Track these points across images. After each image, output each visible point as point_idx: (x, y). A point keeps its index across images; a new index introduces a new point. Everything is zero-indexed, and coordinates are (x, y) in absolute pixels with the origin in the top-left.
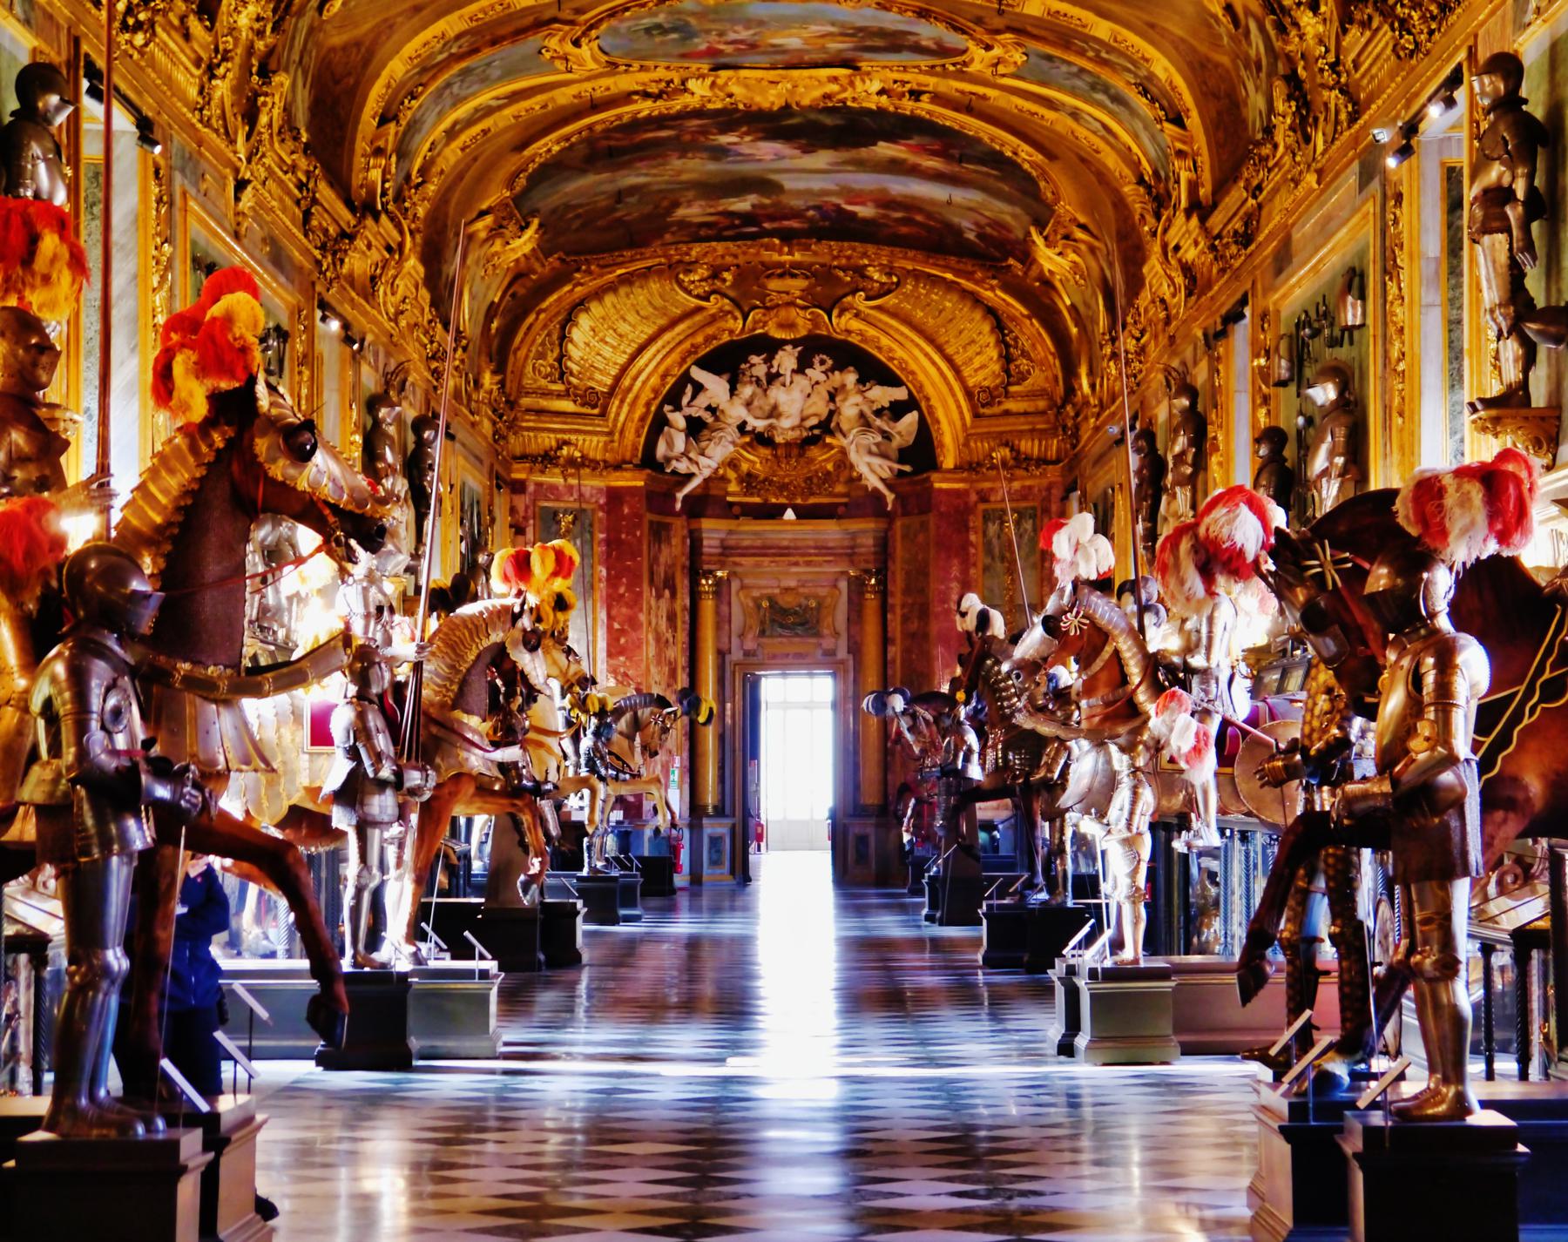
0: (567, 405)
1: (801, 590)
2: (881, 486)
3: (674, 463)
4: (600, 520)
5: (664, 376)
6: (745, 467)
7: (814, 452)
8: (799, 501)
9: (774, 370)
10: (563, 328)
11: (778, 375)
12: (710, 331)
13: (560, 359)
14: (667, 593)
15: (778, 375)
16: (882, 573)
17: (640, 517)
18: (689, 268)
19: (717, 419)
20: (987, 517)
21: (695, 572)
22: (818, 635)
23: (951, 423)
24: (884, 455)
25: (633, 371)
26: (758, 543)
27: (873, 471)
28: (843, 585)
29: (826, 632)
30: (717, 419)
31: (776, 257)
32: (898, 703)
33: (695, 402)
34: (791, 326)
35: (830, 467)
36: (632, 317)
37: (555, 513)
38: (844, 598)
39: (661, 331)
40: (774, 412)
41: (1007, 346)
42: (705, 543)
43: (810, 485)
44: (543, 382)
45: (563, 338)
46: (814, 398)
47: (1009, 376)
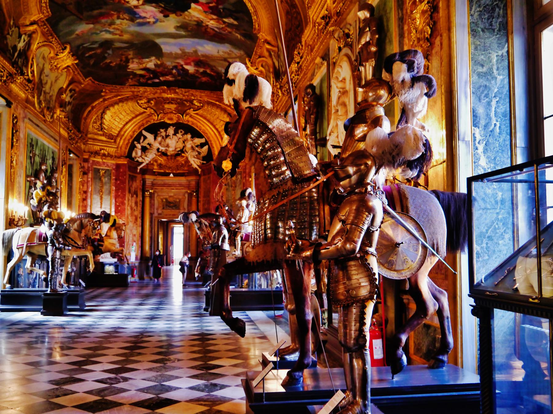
0: (103, 138)
2: (197, 167)
3: (137, 159)
5: (134, 132)
6: (159, 162)
7: (179, 158)
10: (102, 115)
11: (169, 135)
12: (148, 119)
13: (101, 124)
14: (135, 196)
16: (197, 192)
17: (126, 172)
18: (141, 98)
19: (151, 147)
21: (144, 191)
22: (179, 209)
23: (217, 148)
24: (198, 159)
25: (124, 130)
27: (195, 163)
28: (186, 195)
30: (151, 147)
31: (165, 95)
32: (194, 217)
34: (171, 119)
35: (183, 162)
36: (124, 113)
37: (99, 170)
38: (187, 199)
39: (133, 118)
40: (168, 146)
44: (96, 131)
45: (102, 118)
46: (179, 143)
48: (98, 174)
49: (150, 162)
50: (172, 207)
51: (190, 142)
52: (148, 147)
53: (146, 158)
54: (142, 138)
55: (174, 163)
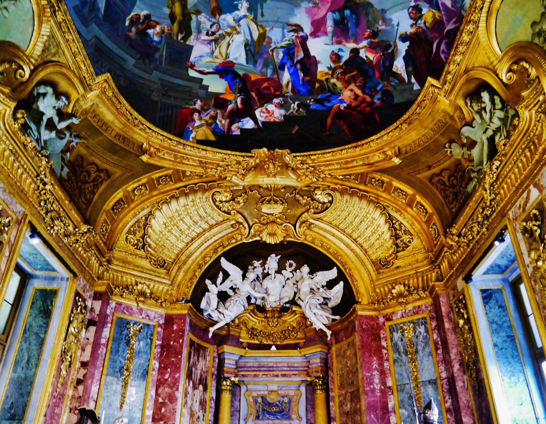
1: (280, 392)
4: (158, 333)
6: (251, 324)
8: (279, 343)
9: (266, 271)
11: (268, 274)
13: (143, 237)
14: (201, 387)
15: (268, 274)
19: (236, 293)
20: (392, 330)
23: (363, 281)
25: (187, 252)
27: (320, 320)
28: (303, 389)
29: (294, 416)
30: (236, 293)
33: (224, 284)
36: (188, 220)
37: (128, 323)
38: (304, 397)
41: (396, 229)
42: (226, 361)
43: (285, 334)
47: (397, 246)
48: (125, 332)
49: (233, 321)
50: (273, 414)
52: (230, 292)
53: (225, 312)
54: (221, 275)
55: (280, 325)
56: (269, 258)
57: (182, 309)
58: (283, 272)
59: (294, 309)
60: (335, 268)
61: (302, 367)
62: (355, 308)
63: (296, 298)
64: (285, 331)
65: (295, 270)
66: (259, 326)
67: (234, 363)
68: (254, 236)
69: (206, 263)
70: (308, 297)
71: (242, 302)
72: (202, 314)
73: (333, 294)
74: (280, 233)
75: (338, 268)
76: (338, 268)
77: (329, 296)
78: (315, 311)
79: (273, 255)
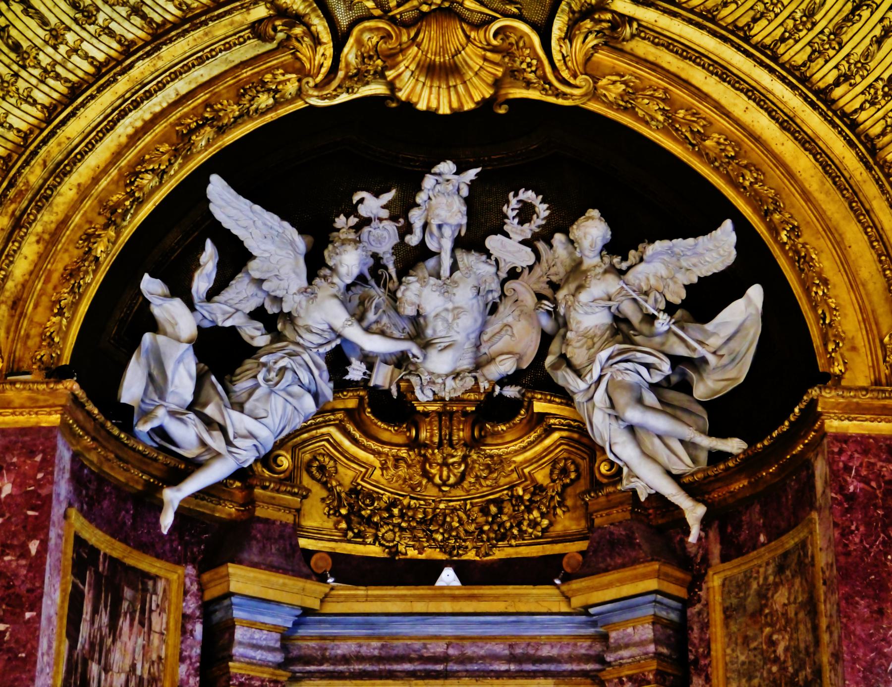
6: (347, 475)
8: (471, 555)
9: (413, 240)
11: (423, 253)
15: (423, 253)
19: (278, 337)
23: (854, 284)
25: (53, 150)
26: (373, 647)
30: (278, 337)
33: (228, 295)
34: (442, 71)
35: (542, 477)
40: (417, 329)
42: (240, 633)
43: (500, 514)
49: (268, 460)
51: (601, 286)
53: (236, 421)
54: (209, 256)
56: (429, 181)
57: (34, 406)
58: (493, 242)
59: (539, 407)
60: (728, 224)
61: (571, 659)
62: (813, 403)
63: (549, 360)
64: (498, 502)
65: (545, 235)
66: (383, 481)
67: (273, 640)
68: (360, 77)
69: (139, 203)
70: (604, 355)
71: (305, 377)
72: (128, 427)
73: (714, 342)
74: (476, 63)
75: (742, 227)
76: (742, 227)
77: (701, 351)
78: (634, 415)
79: (447, 167)
